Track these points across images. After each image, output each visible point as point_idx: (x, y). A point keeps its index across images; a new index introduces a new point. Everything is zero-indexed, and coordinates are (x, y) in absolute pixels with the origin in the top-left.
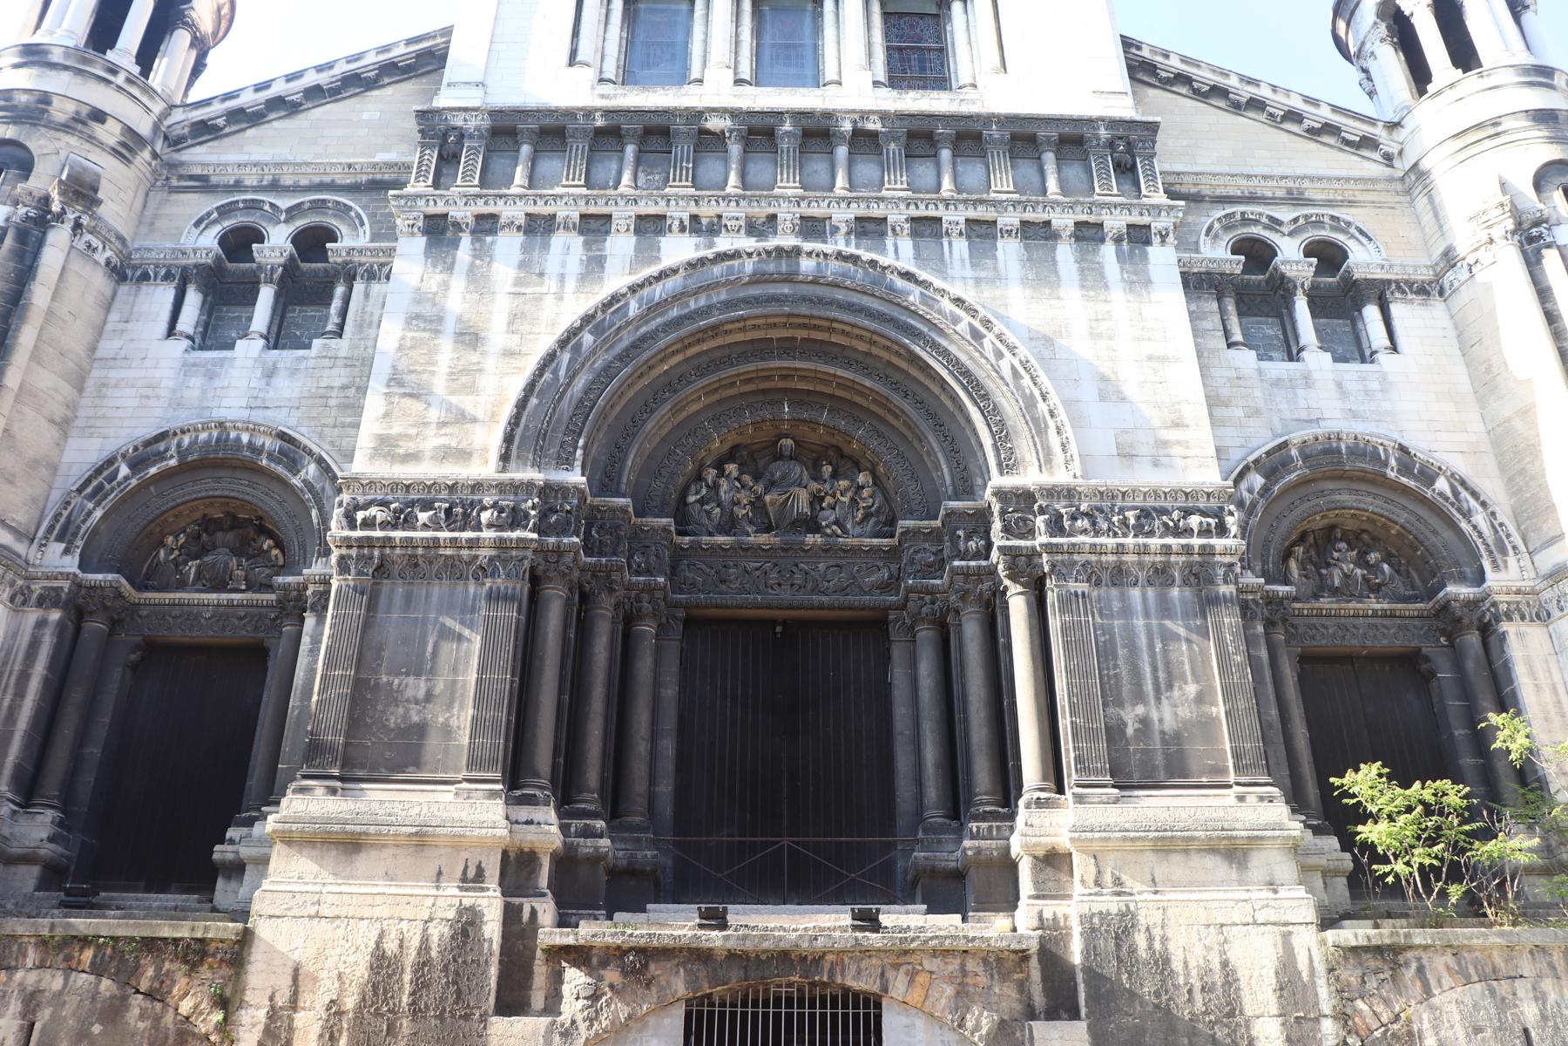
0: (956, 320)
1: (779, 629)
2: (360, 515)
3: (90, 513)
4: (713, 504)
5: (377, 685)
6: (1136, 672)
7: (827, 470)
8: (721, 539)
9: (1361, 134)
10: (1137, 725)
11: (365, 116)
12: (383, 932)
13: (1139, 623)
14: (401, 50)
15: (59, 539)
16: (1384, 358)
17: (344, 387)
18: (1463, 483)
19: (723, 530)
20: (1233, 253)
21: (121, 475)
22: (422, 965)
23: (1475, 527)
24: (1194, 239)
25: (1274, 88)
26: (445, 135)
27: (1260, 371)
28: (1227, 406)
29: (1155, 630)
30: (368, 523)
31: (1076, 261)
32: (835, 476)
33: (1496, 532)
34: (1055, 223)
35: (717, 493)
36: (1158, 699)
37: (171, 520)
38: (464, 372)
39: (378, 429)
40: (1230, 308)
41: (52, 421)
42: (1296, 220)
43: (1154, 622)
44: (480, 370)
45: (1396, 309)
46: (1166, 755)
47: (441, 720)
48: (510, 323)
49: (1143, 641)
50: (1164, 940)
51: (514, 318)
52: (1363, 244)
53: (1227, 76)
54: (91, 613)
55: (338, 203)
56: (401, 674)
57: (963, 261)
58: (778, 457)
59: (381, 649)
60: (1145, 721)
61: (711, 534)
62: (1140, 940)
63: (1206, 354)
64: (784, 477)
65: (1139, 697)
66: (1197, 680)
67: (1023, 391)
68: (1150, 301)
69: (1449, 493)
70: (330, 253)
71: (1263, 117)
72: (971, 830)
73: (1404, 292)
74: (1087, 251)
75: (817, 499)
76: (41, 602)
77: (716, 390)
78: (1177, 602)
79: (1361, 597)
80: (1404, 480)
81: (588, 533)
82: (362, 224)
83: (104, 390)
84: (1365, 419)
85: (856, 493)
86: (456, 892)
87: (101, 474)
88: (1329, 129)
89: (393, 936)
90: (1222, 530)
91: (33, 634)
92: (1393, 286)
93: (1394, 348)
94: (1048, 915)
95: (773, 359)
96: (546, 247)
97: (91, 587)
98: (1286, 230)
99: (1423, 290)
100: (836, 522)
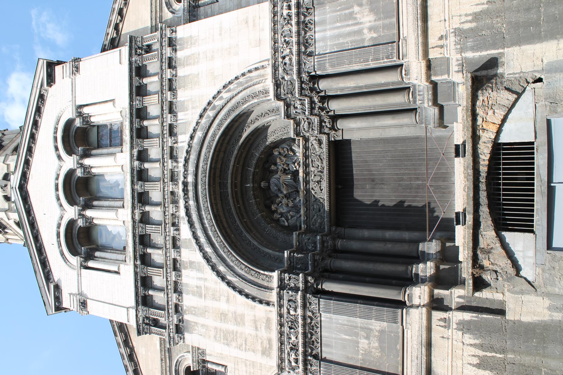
0: (209, 117)
1: (340, 187)
2: (293, 364)
4: (289, 215)
5: (363, 360)
6: (349, 34)
7: (273, 167)
8: (302, 212)
10: (372, 32)
11: (144, 353)
12: (468, 364)
13: (329, 33)
14: (119, 338)
17: (246, 366)
19: (298, 211)
22: (481, 347)
24: (176, 19)
26: (147, 324)
29: (331, 26)
30: (297, 361)
32: (275, 164)
34: (169, 77)
35: (284, 213)
36: (361, 23)
38: (236, 320)
39: (259, 354)
43: (328, 27)
44: (235, 313)
46: (386, 18)
47: (377, 334)
48: (216, 300)
49: (336, 32)
50: (466, 15)
51: (215, 298)
53: (114, 9)
55: (176, 365)
56: (358, 350)
57: (185, 115)
58: (269, 187)
59: (348, 357)
60: (371, 29)
61: (301, 216)
62: (467, 26)
63: (221, 11)
64: (276, 185)
65: (360, 32)
66: (352, 7)
67: (235, 87)
70: (195, 369)
72: (421, 103)
75: (285, 171)
77: (242, 215)
81: (299, 269)
82: (183, 356)
85: (282, 155)
86: (450, 331)
89: (470, 359)
94: (456, 69)
95: (227, 192)
96: (187, 285)
100: (294, 163)
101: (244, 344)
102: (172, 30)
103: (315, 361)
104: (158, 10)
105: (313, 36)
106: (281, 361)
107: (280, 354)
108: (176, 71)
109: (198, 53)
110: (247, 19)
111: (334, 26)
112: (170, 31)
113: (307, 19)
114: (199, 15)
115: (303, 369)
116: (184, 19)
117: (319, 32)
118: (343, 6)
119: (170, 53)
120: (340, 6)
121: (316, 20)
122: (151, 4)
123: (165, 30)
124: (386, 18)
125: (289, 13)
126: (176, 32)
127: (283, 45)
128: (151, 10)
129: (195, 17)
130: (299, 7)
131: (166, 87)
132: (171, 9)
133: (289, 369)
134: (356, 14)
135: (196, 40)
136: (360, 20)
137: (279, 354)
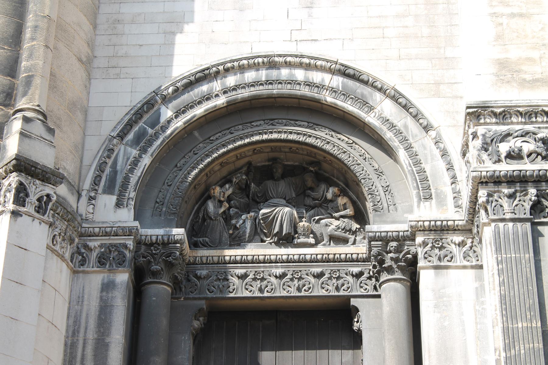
2: (504, 148)
3: (136, 163)
15: (109, 190)
21: (163, 119)
37: (217, 168)
41: (80, 60)
54: (155, 274)
76: (102, 261)
83: (120, 27)
87: (142, 117)
91: (101, 298)
97: (152, 244)
101: (508, 10)
103: (528, 206)
106: (500, 114)
107: (521, 109)
115: (497, 174)
133: (484, 135)
137: (520, 107)
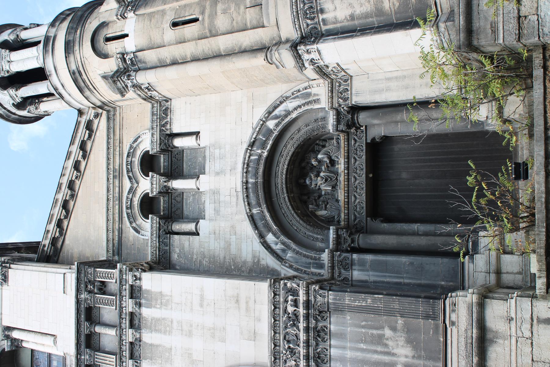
9: (85, 130)
13: (349, 354)
16: (204, 141)
18: (270, 113)
20: (148, 219)
23: (295, 109)
25: (62, 175)
27: (211, 220)
28: (230, 245)
31: (151, 332)
33: (297, 97)
34: (131, 340)
36: (394, 355)
40: (178, 227)
42: (130, 178)
45: (175, 130)
49: (359, 355)
52: (141, 142)
53: (57, 200)
66: (382, 328)
68: (171, 296)
69: (276, 121)
71: (78, 182)
73: (166, 123)
74: (146, 324)
78: (337, 328)
79: (337, 174)
80: (268, 148)
84: (236, 163)
88: (83, 146)
90: (294, 293)
92: (164, 128)
93: (197, 134)
98: (136, 185)
99: (166, 111)
102: (135, 276)
104: (117, 219)
105: (327, 329)
108: (140, 333)
109: (171, 320)
110: (238, 297)
111: (357, 346)
112: (133, 276)
113: (320, 325)
114: (172, 245)
116: (151, 246)
117: (336, 347)
118: (370, 323)
119: (133, 307)
120: (366, 321)
121: (332, 329)
122: (108, 210)
123: (126, 274)
124: (429, 359)
125: (295, 310)
126: (140, 279)
127: (287, 351)
128: (107, 218)
129: (167, 246)
130: (309, 307)
131: (127, 354)
132: (134, 225)
134: (387, 339)
135: (168, 300)
136: (393, 349)
